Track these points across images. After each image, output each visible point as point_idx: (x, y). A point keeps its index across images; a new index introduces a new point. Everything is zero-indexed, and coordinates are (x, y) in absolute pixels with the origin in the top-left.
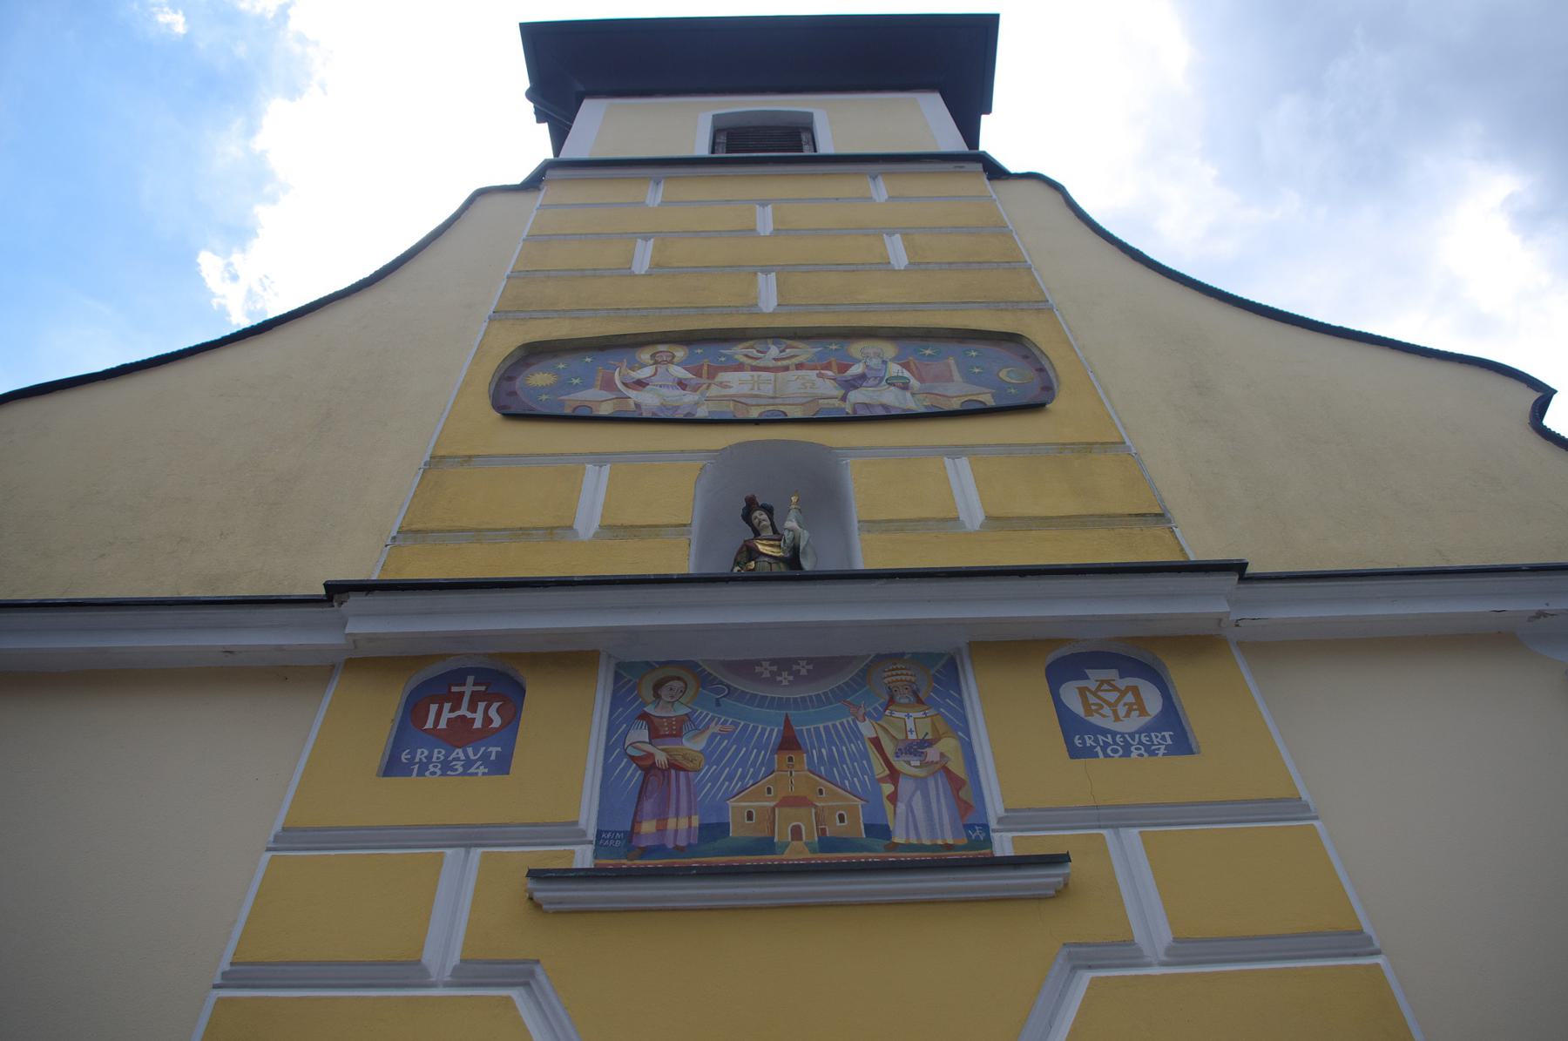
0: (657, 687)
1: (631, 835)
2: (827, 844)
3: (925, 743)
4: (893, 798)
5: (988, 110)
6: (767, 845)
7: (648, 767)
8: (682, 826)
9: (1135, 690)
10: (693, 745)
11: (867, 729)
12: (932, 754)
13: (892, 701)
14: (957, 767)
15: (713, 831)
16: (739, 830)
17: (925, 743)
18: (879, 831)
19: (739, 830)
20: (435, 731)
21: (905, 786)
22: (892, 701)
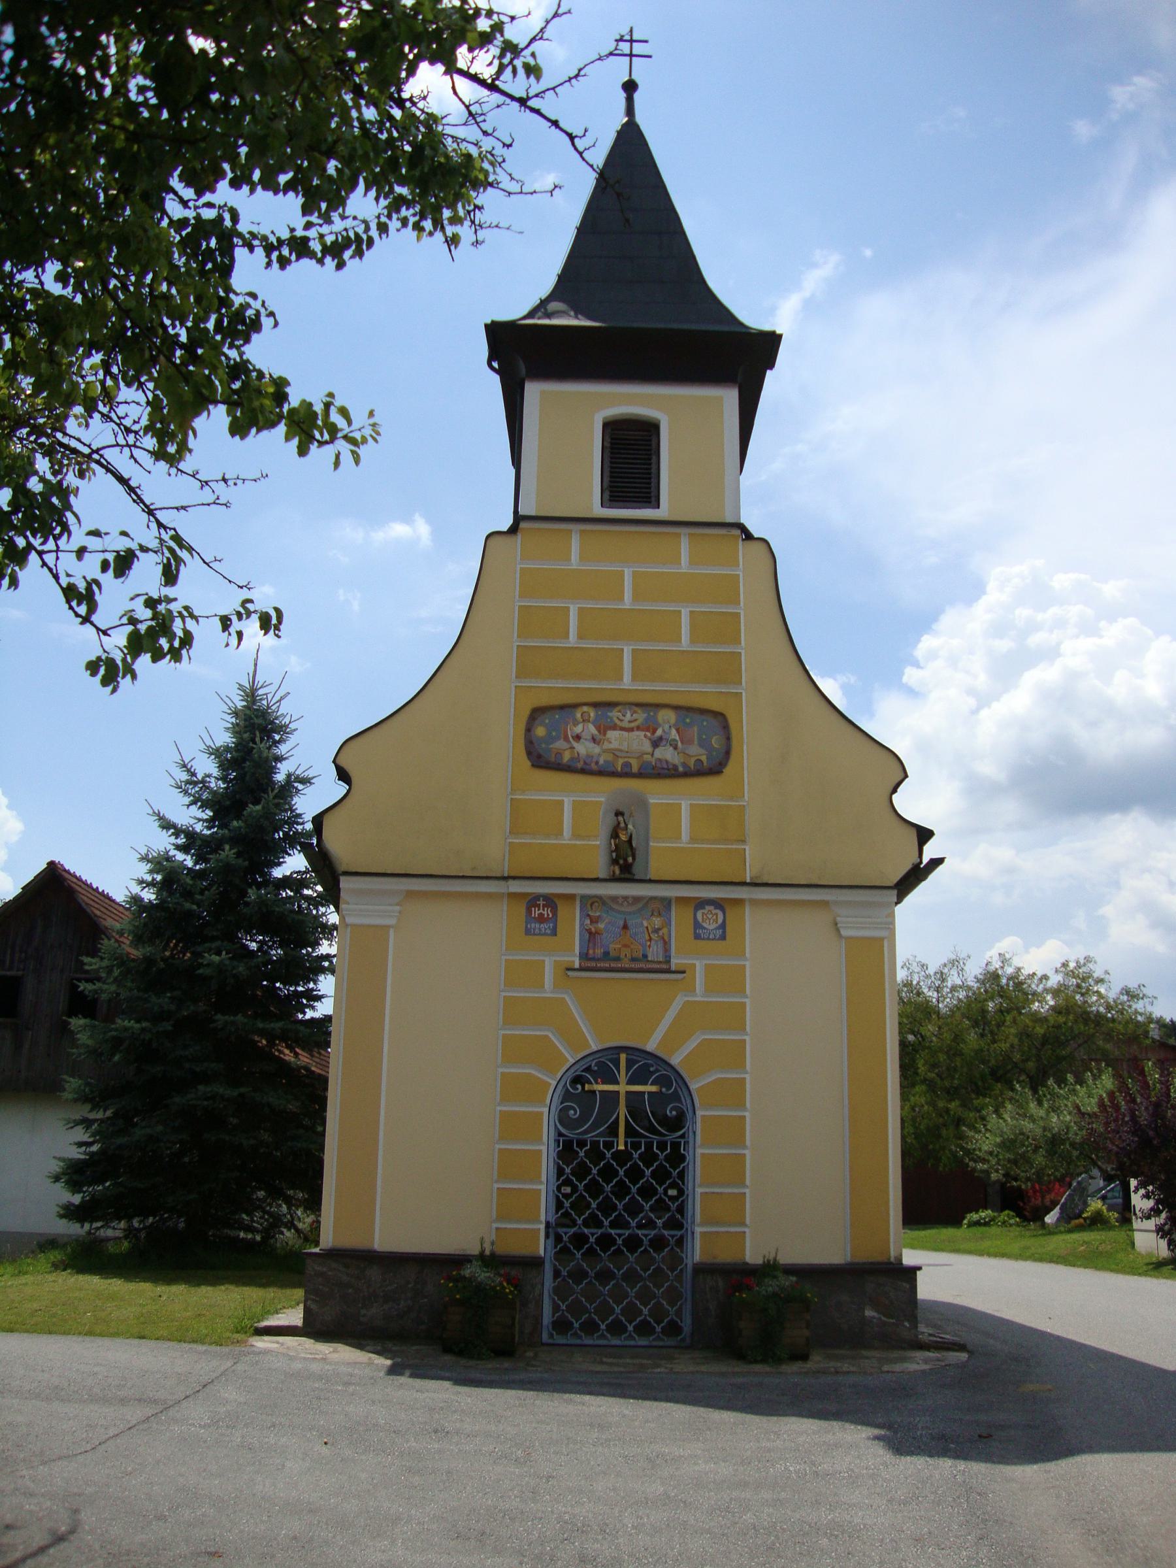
0: (591, 905)
1: (587, 954)
2: (633, 960)
3: (659, 929)
4: (649, 946)
5: (771, 366)
6: (618, 959)
7: (590, 933)
8: (599, 952)
9: (717, 914)
10: (601, 926)
11: (645, 923)
12: (661, 933)
13: (652, 915)
14: (666, 938)
15: (606, 954)
16: (613, 954)
17: (659, 929)
18: (645, 956)
19: (613, 954)
20: (535, 918)
21: (653, 942)
22: (652, 915)
